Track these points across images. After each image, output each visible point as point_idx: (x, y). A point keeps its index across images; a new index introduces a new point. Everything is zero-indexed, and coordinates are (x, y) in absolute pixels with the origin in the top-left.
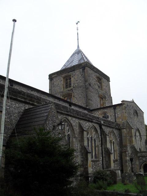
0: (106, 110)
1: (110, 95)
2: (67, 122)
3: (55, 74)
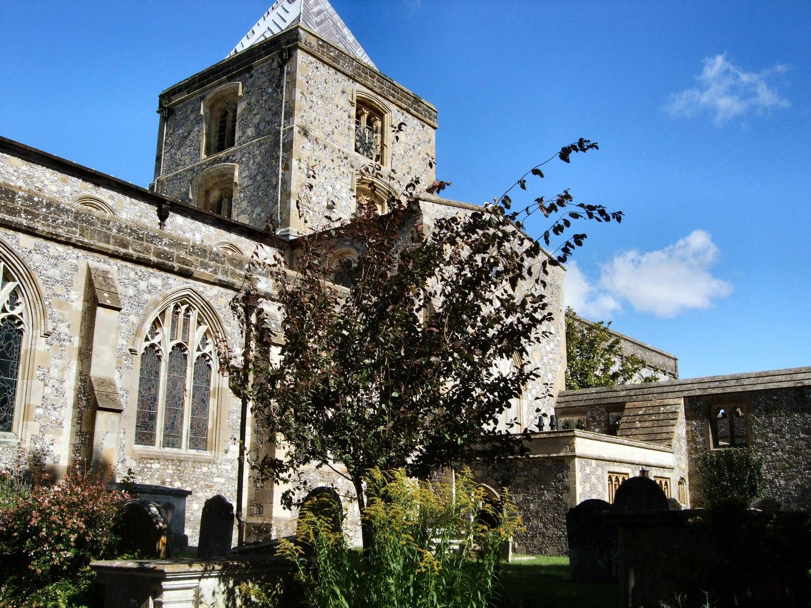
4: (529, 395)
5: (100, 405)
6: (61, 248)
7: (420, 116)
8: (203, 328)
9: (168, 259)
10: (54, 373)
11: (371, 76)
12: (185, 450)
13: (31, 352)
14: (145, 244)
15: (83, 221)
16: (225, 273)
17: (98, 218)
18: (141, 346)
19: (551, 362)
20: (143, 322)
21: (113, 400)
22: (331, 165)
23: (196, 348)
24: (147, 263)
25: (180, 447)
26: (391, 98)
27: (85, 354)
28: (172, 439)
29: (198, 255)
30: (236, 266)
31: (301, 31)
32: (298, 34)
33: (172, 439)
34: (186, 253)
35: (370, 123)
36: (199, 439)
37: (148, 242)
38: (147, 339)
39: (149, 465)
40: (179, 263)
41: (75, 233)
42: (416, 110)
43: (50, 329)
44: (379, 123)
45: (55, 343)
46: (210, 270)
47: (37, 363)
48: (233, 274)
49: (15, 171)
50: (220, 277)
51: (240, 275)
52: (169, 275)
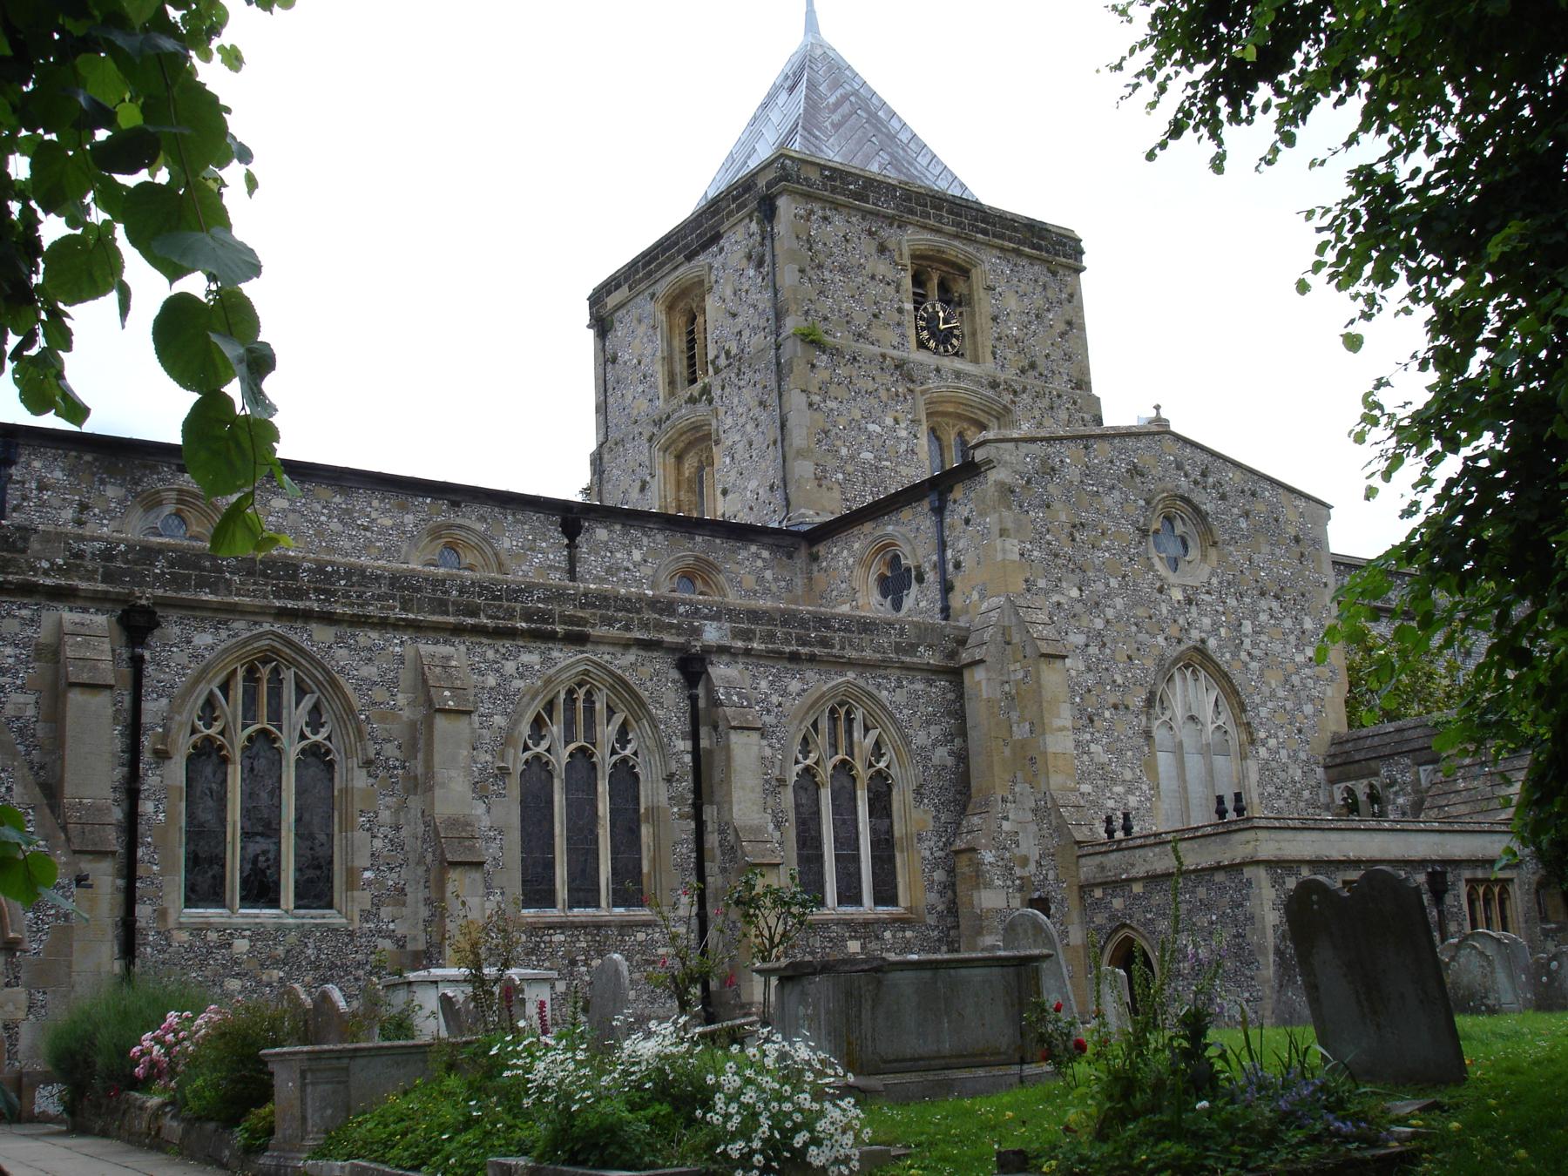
0: (890, 528)
1: (1082, 383)
2: (292, 663)
3: (618, 286)
4: (1263, 752)
5: (450, 857)
6: (374, 635)
8: (618, 719)
9: (546, 621)
10: (385, 816)
12: (607, 911)
13: (346, 791)
14: (506, 604)
15: (403, 588)
16: (645, 626)
17: (426, 579)
18: (516, 761)
19: (1310, 683)
20: (514, 724)
21: (471, 848)
23: (608, 751)
24: (512, 633)
25: (598, 906)
27: (421, 784)
28: (584, 892)
29: (595, 606)
33: (584, 892)
34: (575, 606)
35: (944, 287)
36: (629, 889)
37: (510, 601)
38: (526, 748)
39: (547, 938)
40: (565, 624)
41: (392, 608)
42: (1034, 247)
43: (372, 755)
45: (382, 773)
47: (358, 806)
48: (660, 627)
49: (324, 507)
51: (671, 626)
52: (550, 645)
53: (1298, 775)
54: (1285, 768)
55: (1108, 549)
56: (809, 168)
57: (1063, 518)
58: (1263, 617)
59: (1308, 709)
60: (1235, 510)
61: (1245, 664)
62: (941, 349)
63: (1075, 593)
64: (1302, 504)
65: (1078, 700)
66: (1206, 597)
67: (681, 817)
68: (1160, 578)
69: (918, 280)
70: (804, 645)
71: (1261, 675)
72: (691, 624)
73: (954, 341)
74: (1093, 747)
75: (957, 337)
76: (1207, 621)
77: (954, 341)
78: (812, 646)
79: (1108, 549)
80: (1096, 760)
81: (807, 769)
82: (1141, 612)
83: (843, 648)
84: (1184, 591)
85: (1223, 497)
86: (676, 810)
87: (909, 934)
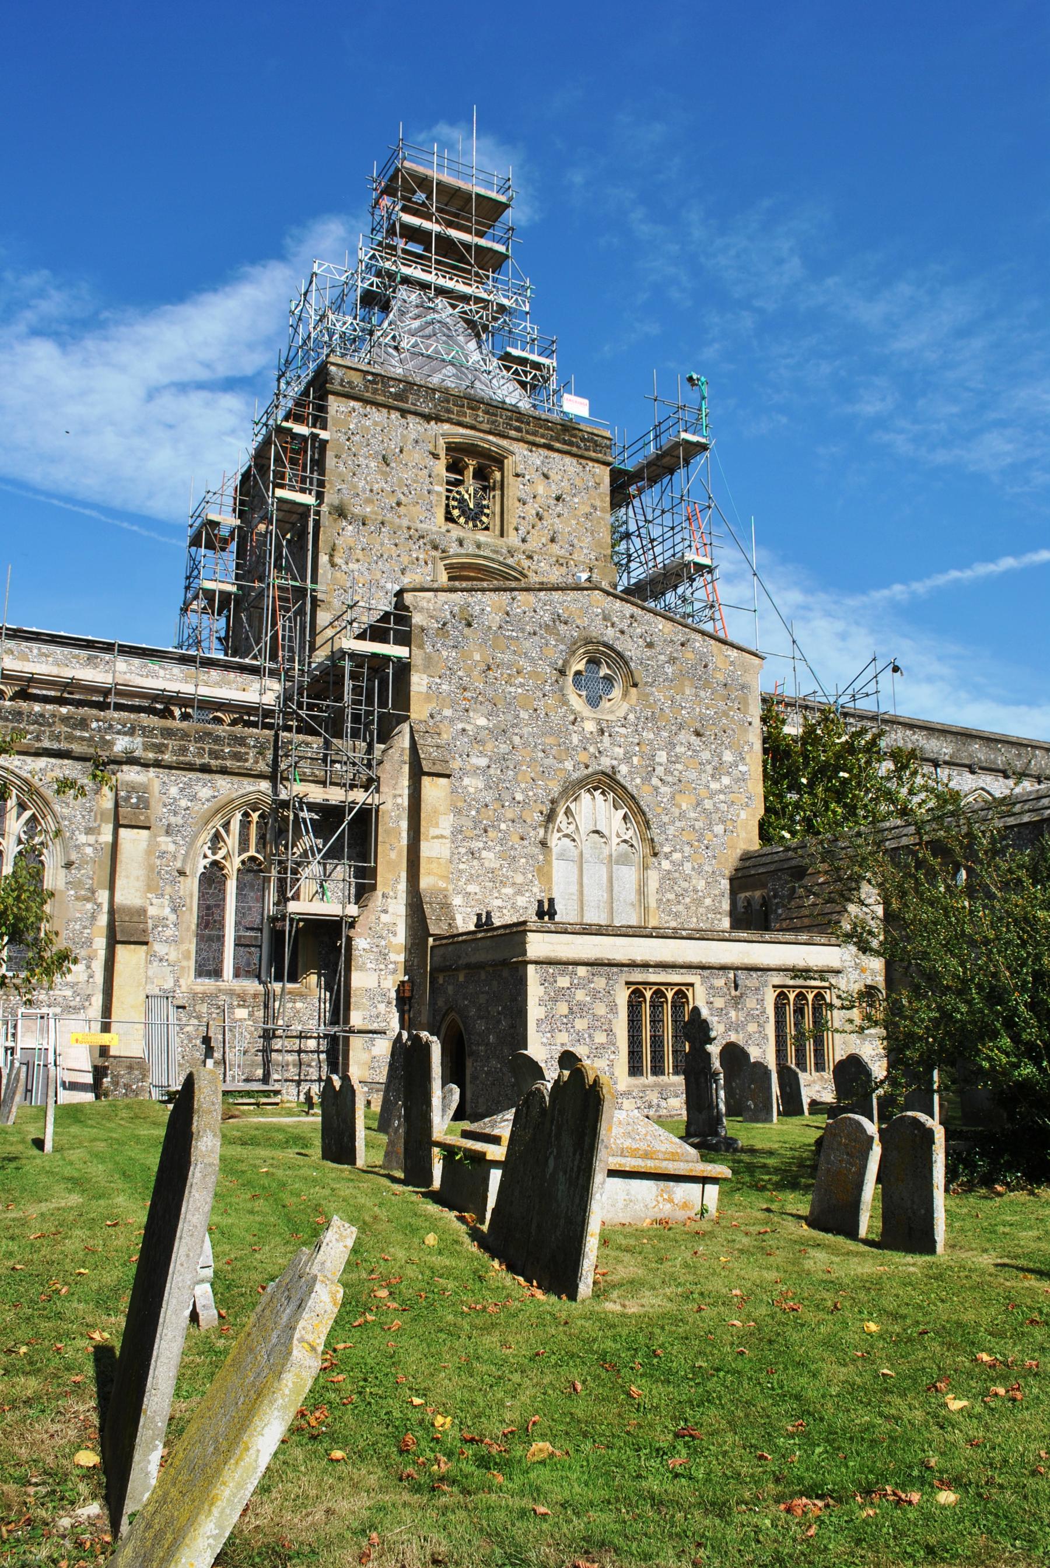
7: (574, 450)
11: (472, 409)
16: (57, 738)
19: (724, 807)
22: (394, 552)
26: (513, 433)
30: (74, 727)
31: (333, 368)
32: (328, 373)
42: (565, 442)
44: (498, 475)
46: (29, 737)
48: (70, 738)
50: (46, 744)
51: (83, 739)
53: (701, 885)
54: (687, 879)
55: (522, 685)
56: (352, 372)
57: (477, 657)
58: (680, 749)
59: (719, 829)
60: (662, 657)
61: (656, 789)
62: (471, 524)
63: (482, 722)
64: (734, 653)
65: (473, 813)
66: (623, 731)
67: (77, 899)
68: (573, 712)
69: (454, 467)
70: (216, 758)
71: (673, 798)
72: (102, 738)
73: (484, 519)
74: (484, 854)
75: (487, 516)
76: (619, 751)
77: (484, 519)
78: (224, 759)
79: (522, 685)
80: (486, 864)
81: (215, 863)
82: (550, 740)
83: (257, 762)
84: (599, 723)
85: (650, 645)
86: (72, 892)
87: (299, 1005)
